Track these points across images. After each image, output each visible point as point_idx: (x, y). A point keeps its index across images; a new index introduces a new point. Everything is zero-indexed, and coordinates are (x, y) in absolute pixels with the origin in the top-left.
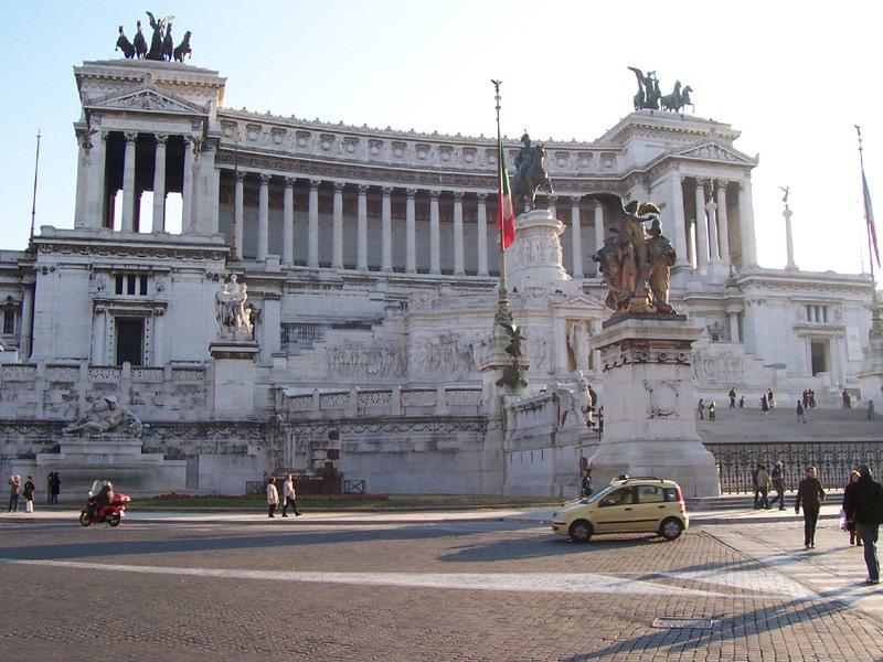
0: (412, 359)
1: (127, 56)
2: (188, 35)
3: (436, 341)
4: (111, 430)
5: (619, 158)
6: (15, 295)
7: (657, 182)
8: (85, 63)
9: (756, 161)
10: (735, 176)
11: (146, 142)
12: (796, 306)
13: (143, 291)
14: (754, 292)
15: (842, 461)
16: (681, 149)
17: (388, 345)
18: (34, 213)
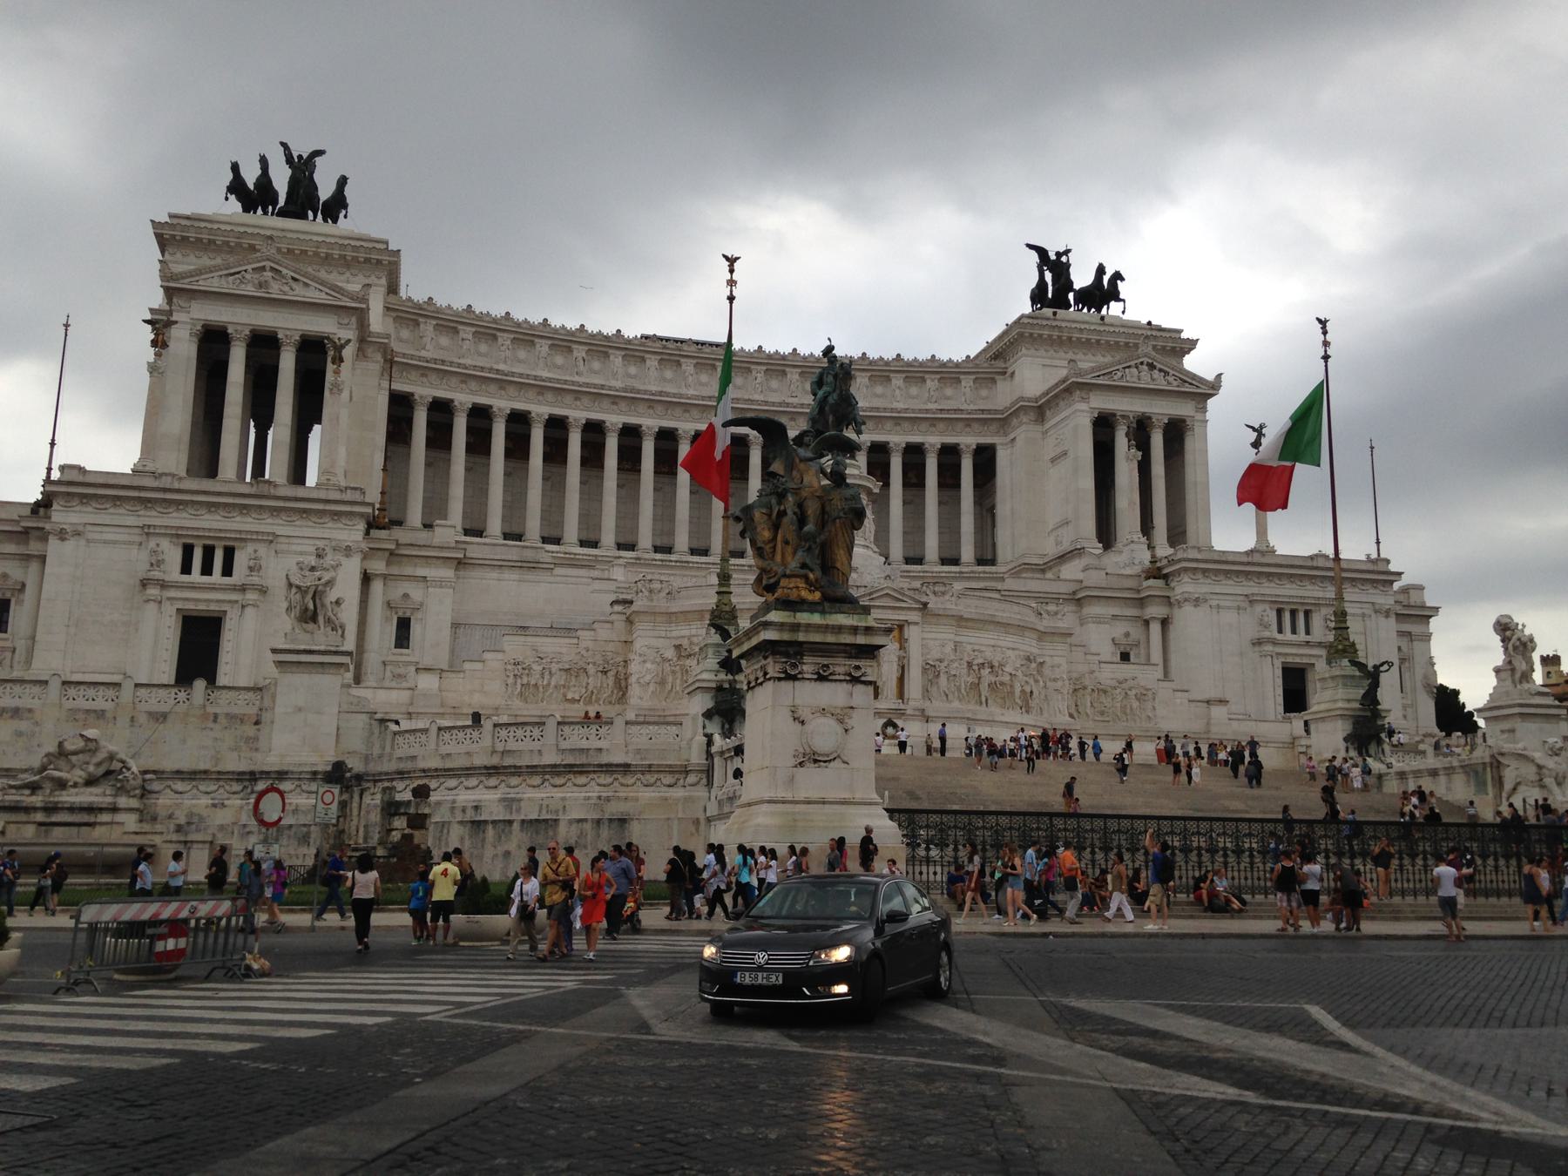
0: (633, 680)
1: (246, 209)
2: (343, 181)
3: (670, 653)
4: (90, 782)
5: (1002, 386)
6: (14, 571)
7: (1058, 419)
8: (171, 216)
9: (1214, 386)
10: (1182, 409)
11: (264, 345)
12: (1259, 608)
14: (1185, 587)
15: (1225, 849)
16: (1093, 370)
18: (53, 444)
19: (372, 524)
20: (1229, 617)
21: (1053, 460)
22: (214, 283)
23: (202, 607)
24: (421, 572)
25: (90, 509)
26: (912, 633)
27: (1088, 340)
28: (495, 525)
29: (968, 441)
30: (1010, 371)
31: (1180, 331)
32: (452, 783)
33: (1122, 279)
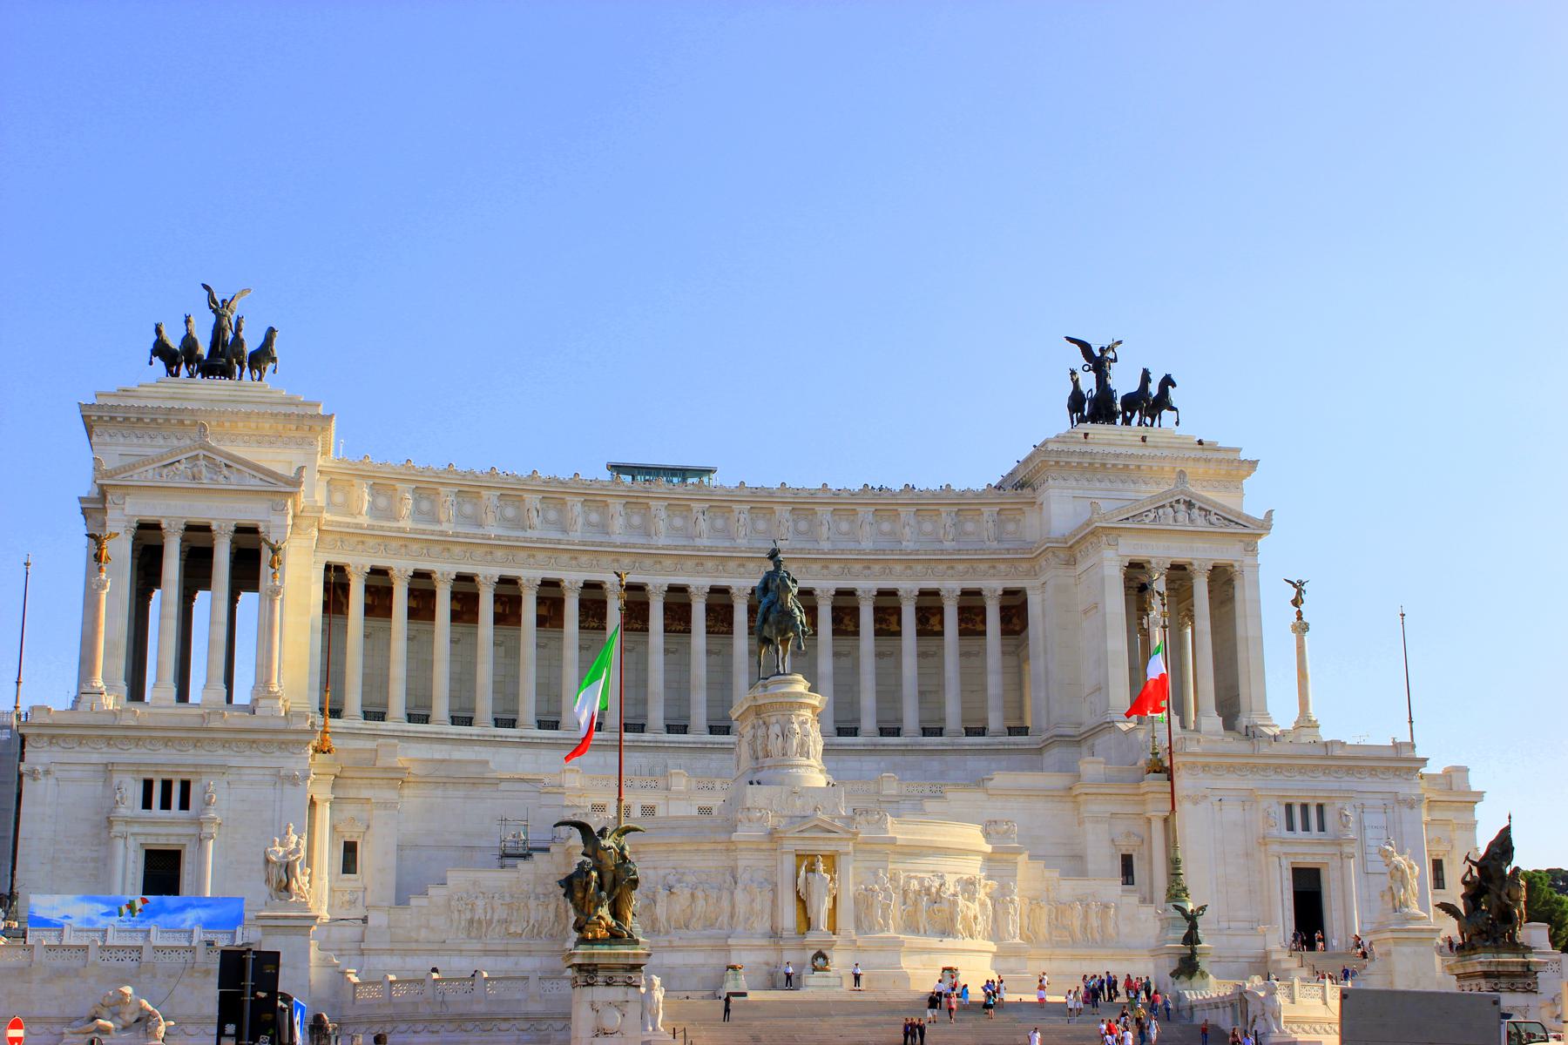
2: (271, 331)
4: (125, 1028)
5: (1031, 520)
9: (1265, 525)
13: (184, 805)
17: (540, 890)
19: (316, 750)
20: (1233, 812)
21: (1085, 612)
22: (148, 475)
23: (162, 840)
24: (365, 794)
25: (55, 749)
26: (842, 862)
27: (1126, 466)
28: (441, 707)
29: (992, 586)
30: (1039, 501)
31: (1238, 450)
32: (403, 1027)
33: (1174, 385)
